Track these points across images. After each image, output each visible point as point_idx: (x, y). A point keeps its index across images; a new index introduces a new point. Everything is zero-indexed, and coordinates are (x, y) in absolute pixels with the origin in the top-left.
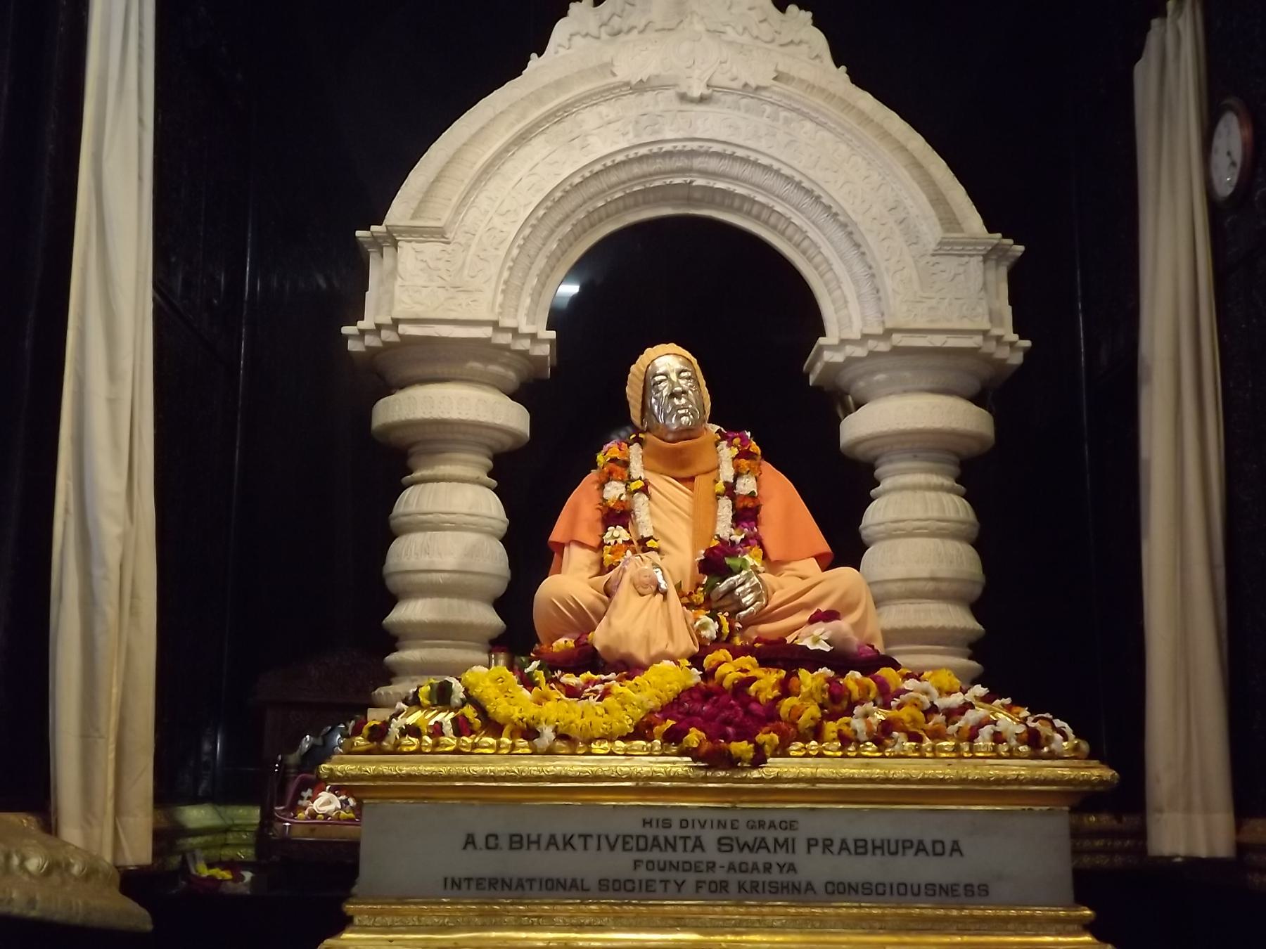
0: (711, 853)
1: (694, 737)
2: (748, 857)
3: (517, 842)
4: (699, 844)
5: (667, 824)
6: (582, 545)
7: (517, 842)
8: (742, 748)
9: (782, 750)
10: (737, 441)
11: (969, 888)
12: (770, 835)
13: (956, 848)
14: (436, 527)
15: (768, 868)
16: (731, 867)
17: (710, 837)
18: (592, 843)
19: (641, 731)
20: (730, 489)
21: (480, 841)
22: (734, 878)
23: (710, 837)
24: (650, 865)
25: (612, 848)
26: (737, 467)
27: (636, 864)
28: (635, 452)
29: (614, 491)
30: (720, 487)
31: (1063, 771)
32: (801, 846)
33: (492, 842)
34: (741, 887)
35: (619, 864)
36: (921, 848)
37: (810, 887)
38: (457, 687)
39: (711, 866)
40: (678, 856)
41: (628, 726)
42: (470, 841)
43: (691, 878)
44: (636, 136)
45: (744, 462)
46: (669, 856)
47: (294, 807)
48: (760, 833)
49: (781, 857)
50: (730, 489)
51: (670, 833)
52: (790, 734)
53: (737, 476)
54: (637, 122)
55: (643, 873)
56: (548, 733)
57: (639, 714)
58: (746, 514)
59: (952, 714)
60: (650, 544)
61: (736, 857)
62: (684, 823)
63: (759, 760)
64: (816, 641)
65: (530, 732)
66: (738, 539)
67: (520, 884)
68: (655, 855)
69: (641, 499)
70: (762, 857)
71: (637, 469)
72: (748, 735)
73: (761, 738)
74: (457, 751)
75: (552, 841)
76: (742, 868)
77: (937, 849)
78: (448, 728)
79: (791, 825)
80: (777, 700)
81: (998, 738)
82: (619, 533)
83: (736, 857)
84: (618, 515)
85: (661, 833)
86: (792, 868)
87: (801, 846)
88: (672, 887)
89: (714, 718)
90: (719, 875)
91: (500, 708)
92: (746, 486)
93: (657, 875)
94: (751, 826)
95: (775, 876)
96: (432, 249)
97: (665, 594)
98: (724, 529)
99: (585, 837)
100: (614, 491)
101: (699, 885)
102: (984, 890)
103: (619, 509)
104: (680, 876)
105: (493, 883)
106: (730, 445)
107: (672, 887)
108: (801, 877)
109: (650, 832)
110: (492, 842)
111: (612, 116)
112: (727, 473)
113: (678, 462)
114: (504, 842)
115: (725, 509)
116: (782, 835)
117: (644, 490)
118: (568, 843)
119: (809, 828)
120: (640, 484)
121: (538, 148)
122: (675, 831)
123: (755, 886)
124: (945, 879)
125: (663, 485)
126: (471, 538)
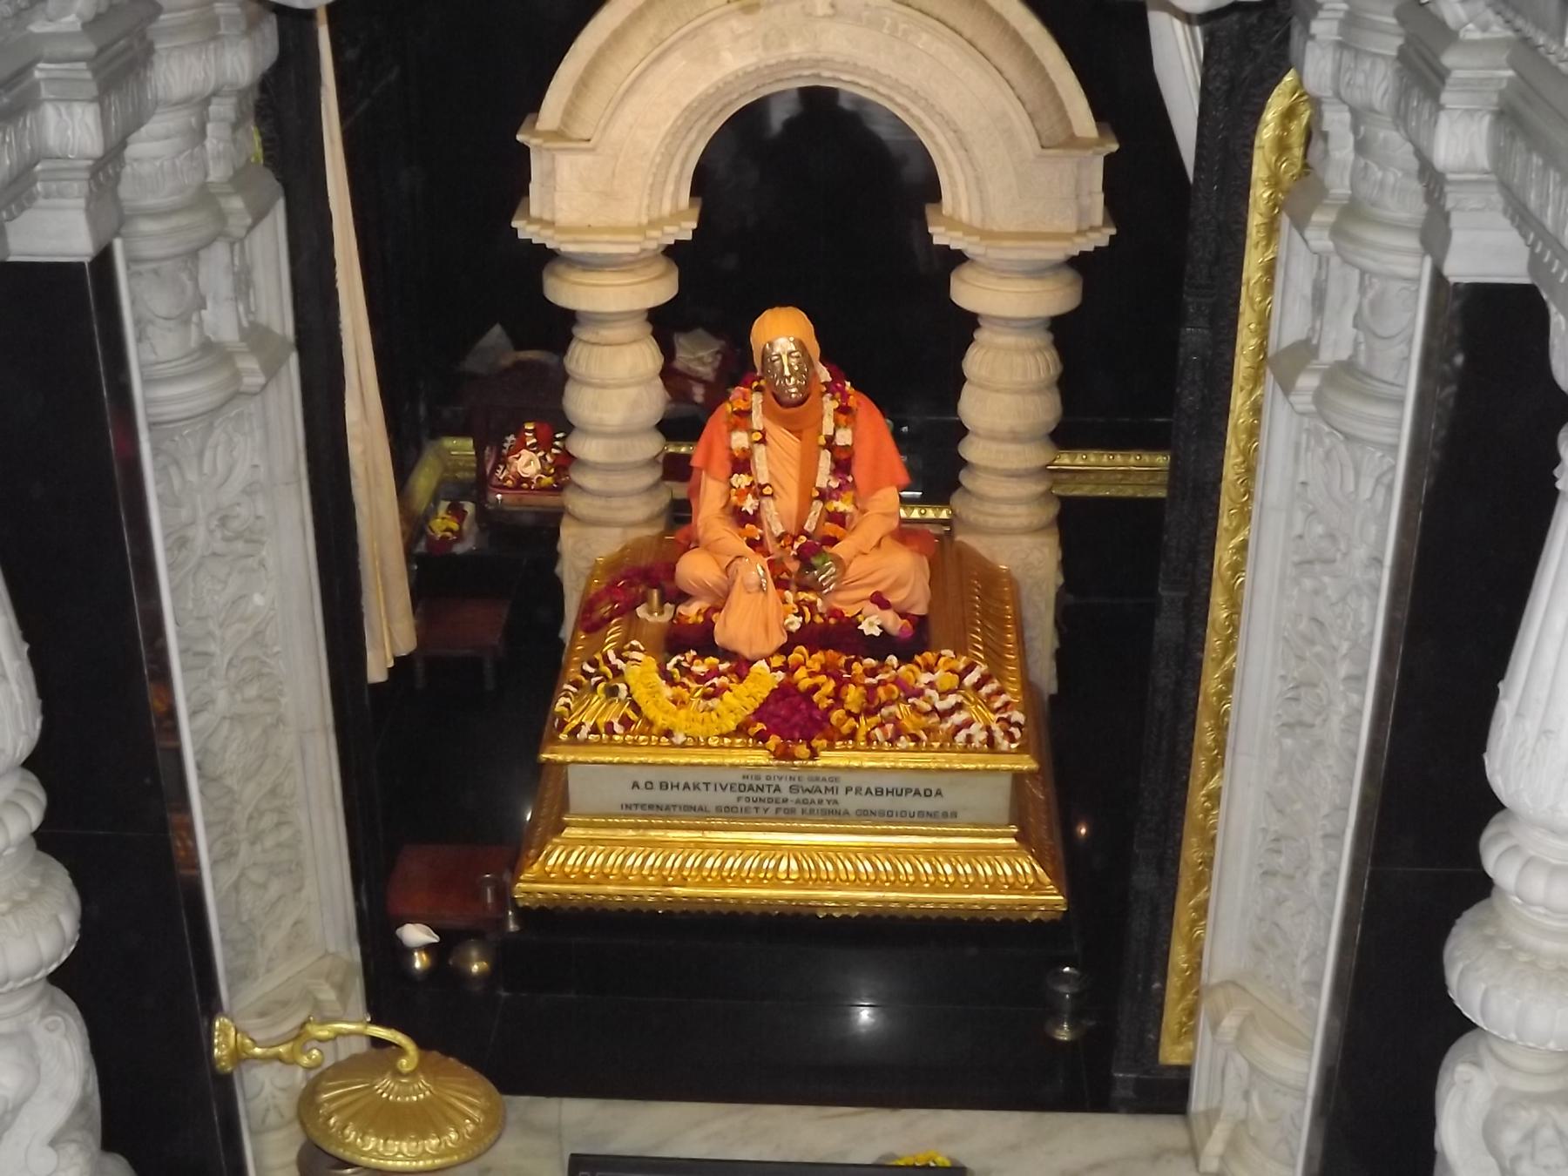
0: (785, 793)
1: (774, 741)
2: (808, 796)
3: (664, 786)
4: (778, 789)
5: (758, 778)
6: (715, 478)
7: (664, 786)
8: (802, 750)
9: (831, 748)
10: (838, 395)
11: (945, 815)
12: (822, 786)
13: (939, 793)
14: (603, 387)
15: (820, 802)
16: (798, 802)
17: (785, 785)
18: (711, 787)
19: (741, 730)
20: (830, 440)
21: (642, 785)
22: (799, 808)
23: (785, 785)
24: (748, 799)
25: (724, 789)
26: (836, 421)
27: (739, 799)
28: (756, 399)
29: (740, 440)
30: (822, 441)
31: (1006, 764)
32: (842, 791)
33: (649, 785)
34: (803, 811)
35: (729, 798)
36: (917, 793)
37: (847, 813)
38: (622, 687)
39: (785, 801)
40: (765, 795)
41: (732, 726)
42: (635, 785)
43: (773, 806)
44: (766, 48)
45: (842, 418)
46: (759, 794)
47: (502, 460)
48: (816, 784)
49: (829, 796)
50: (830, 440)
51: (760, 783)
52: (835, 737)
53: (837, 426)
54: (766, 36)
55: (743, 804)
56: (679, 738)
57: (740, 718)
58: (843, 464)
59: (944, 715)
60: (767, 491)
61: (801, 796)
62: (768, 778)
63: (814, 755)
64: (871, 624)
65: (668, 733)
66: (834, 484)
67: (668, 808)
68: (751, 794)
69: (760, 451)
70: (817, 796)
71: (757, 420)
72: (808, 740)
73: (816, 743)
74: (624, 744)
75: (686, 786)
76: (805, 802)
77: (928, 793)
78: (618, 728)
79: (836, 779)
80: (830, 709)
81: (969, 738)
82: (742, 480)
83: (801, 796)
84: (742, 464)
85: (755, 783)
86: (836, 802)
87: (842, 791)
88: (761, 812)
89: (791, 719)
90: (790, 805)
91: (650, 711)
92: (844, 438)
93: (752, 804)
94: (810, 779)
95: (825, 806)
96: (584, 159)
97: (766, 593)
98: (824, 479)
99: (707, 784)
100: (740, 440)
101: (777, 810)
102: (954, 815)
103: (742, 457)
104: (766, 805)
105: (651, 807)
106: (832, 398)
107: (761, 812)
108: (842, 806)
109: (747, 782)
110: (649, 785)
111: (741, 30)
112: (828, 426)
113: (792, 410)
114: (657, 786)
115: (825, 461)
116: (830, 785)
117: (763, 441)
118: (696, 787)
119: (847, 780)
120: (758, 437)
121: (676, 64)
122: (763, 781)
123: (812, 811)
124: (931, 809)
125: (778, 434)
126: (632, 392)
